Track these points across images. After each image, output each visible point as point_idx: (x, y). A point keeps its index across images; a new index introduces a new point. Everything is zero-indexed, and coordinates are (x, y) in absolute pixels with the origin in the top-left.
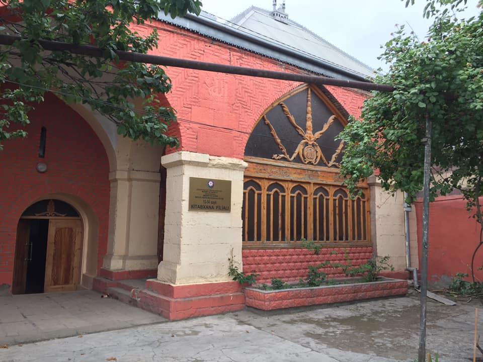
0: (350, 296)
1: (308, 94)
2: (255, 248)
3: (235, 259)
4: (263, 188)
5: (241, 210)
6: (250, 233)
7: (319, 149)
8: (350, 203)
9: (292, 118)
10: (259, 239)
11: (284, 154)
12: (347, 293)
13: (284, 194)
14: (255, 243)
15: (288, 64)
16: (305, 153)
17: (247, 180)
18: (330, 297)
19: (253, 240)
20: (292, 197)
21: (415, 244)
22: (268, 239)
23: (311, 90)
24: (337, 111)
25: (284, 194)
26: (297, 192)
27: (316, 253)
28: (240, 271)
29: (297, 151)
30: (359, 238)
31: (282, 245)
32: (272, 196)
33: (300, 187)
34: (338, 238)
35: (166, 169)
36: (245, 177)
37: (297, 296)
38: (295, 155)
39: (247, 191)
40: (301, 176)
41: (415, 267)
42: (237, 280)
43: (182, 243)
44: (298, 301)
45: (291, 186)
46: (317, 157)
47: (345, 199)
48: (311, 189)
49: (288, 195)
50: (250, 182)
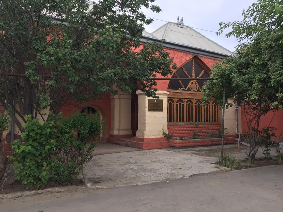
0: (210, 143)
1: (193, 62)
2: (172, 125)
3: (165, 129)
4: (175, 102)
5: (167, 110)
6: (170, 119)
7: (197, 85)
8: (211, 107)
9: (186, 73)
10: (174, 121)
11: (183, 87)
12: (208, 142)
13: (183, 104)
14: (172, 123)
15: (184, 51)
16: (192, 87)
17: (169, 99)
18: (201, 143)
19: (171, 122)
20: (187, 105)
21: (240, 123)
22: (177, 121)
23: (194, 60)
24: (206, 68)
25: (183, 104)
26: (189, 103)
27: (196, 127)
28: (167, 133)
29: (188, 86)
30: (215, 121)
31: (183, 124)
32: (178, 105)
33: (190, 100)
34: (206, 121)
35: (138, 96)
36: (168, 98)
37: (189, 142)
38: (187, 88)
39: (169, 103)
40: (190, 96)
41: (240, 132)
42: (166, 137)
43: (146, 123)
44: (189, 144)
45: (186, 100)
46: (197, 88)
47: (209, 105)
48: (194, 102)
49: (185, 104)
50: (170, 100)
